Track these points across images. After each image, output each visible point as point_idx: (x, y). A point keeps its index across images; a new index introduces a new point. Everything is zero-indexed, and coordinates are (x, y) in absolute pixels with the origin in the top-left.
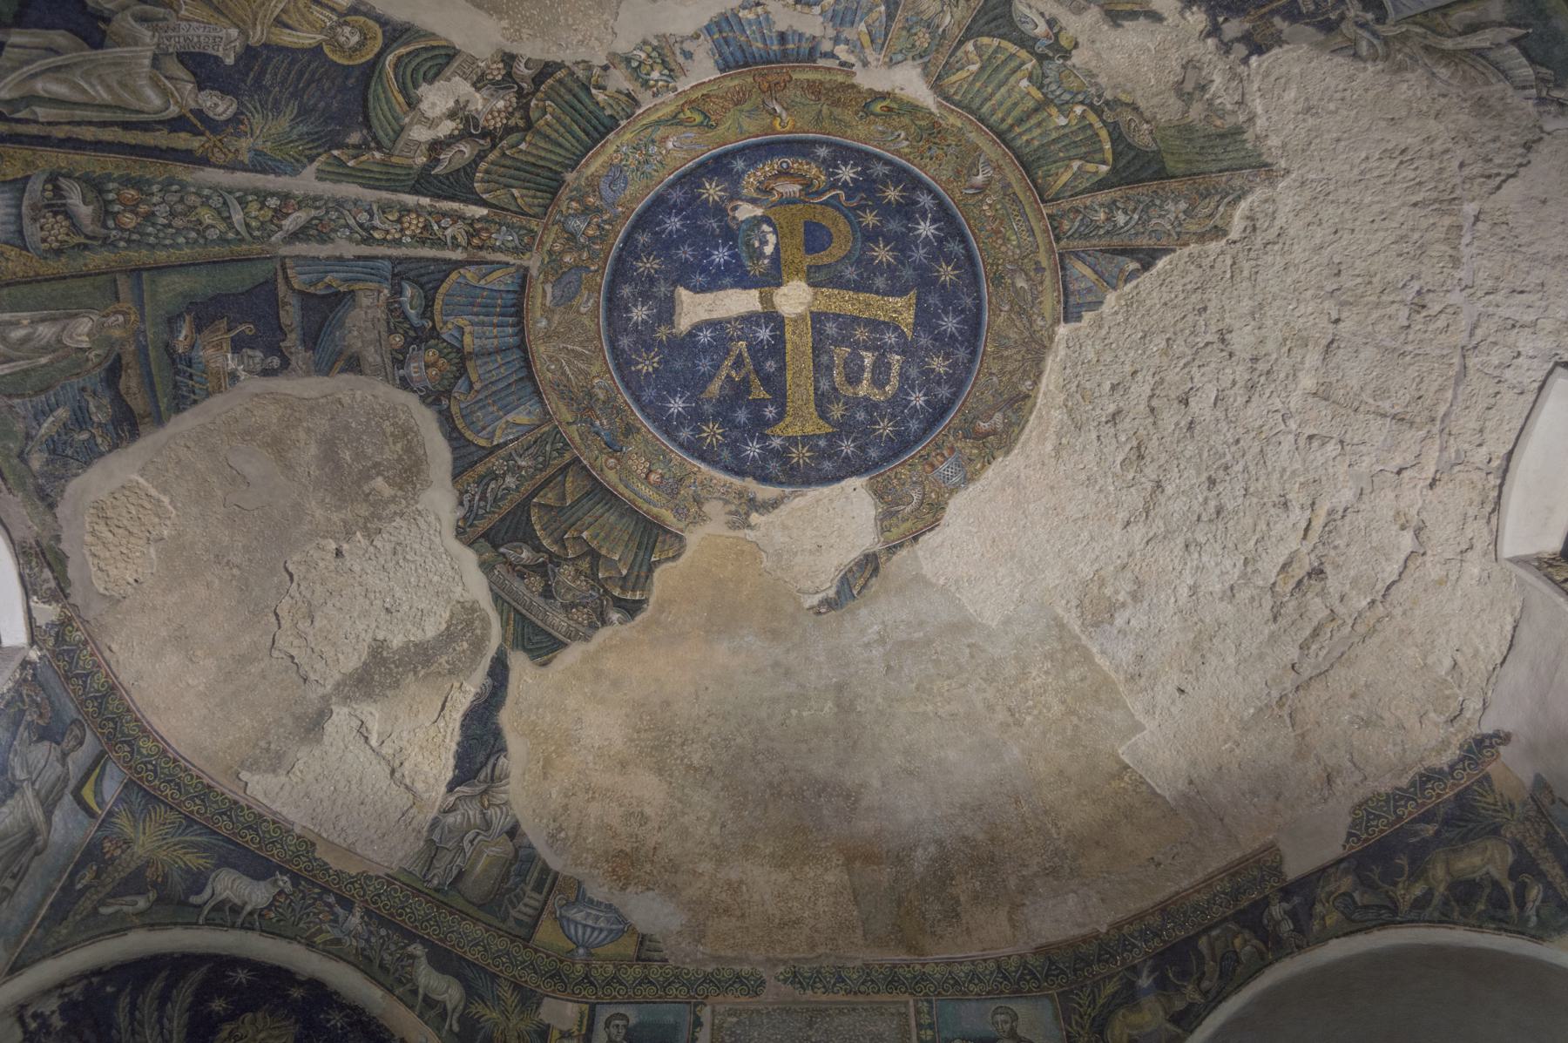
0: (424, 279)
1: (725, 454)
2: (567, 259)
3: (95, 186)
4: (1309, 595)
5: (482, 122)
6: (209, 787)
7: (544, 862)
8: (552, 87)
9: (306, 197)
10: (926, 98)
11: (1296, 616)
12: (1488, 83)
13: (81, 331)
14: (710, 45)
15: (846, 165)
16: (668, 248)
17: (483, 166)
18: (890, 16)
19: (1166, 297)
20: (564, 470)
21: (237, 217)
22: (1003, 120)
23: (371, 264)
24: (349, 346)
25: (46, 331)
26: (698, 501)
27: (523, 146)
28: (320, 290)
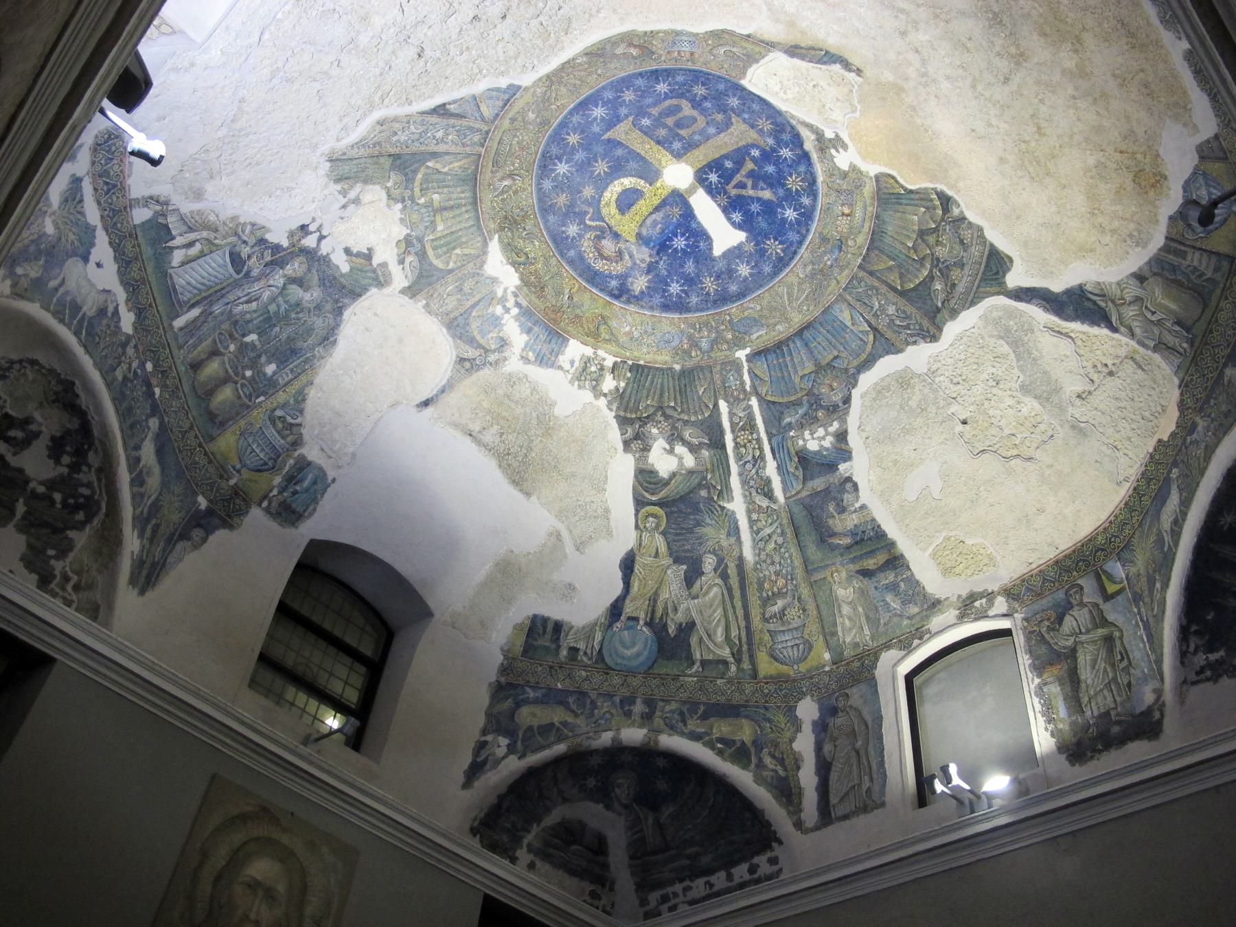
0: (777, 414)
1: (802, 168)
3: (766, 601)
6: (1126, 504)
7: (1160, 249)
8: (631, 412)
10: (494, 247)
12: (192, 212)
13: (844, 593)
14: (561, 358)
15: (568, 237)
16: (692, 279)
18: (473, 306)
19: (443, 81)
20: (871, 274)
21: (768, 531)
25: (846, 610)
26: (845, 175)
27: (672, 404)
28: (800, 473)
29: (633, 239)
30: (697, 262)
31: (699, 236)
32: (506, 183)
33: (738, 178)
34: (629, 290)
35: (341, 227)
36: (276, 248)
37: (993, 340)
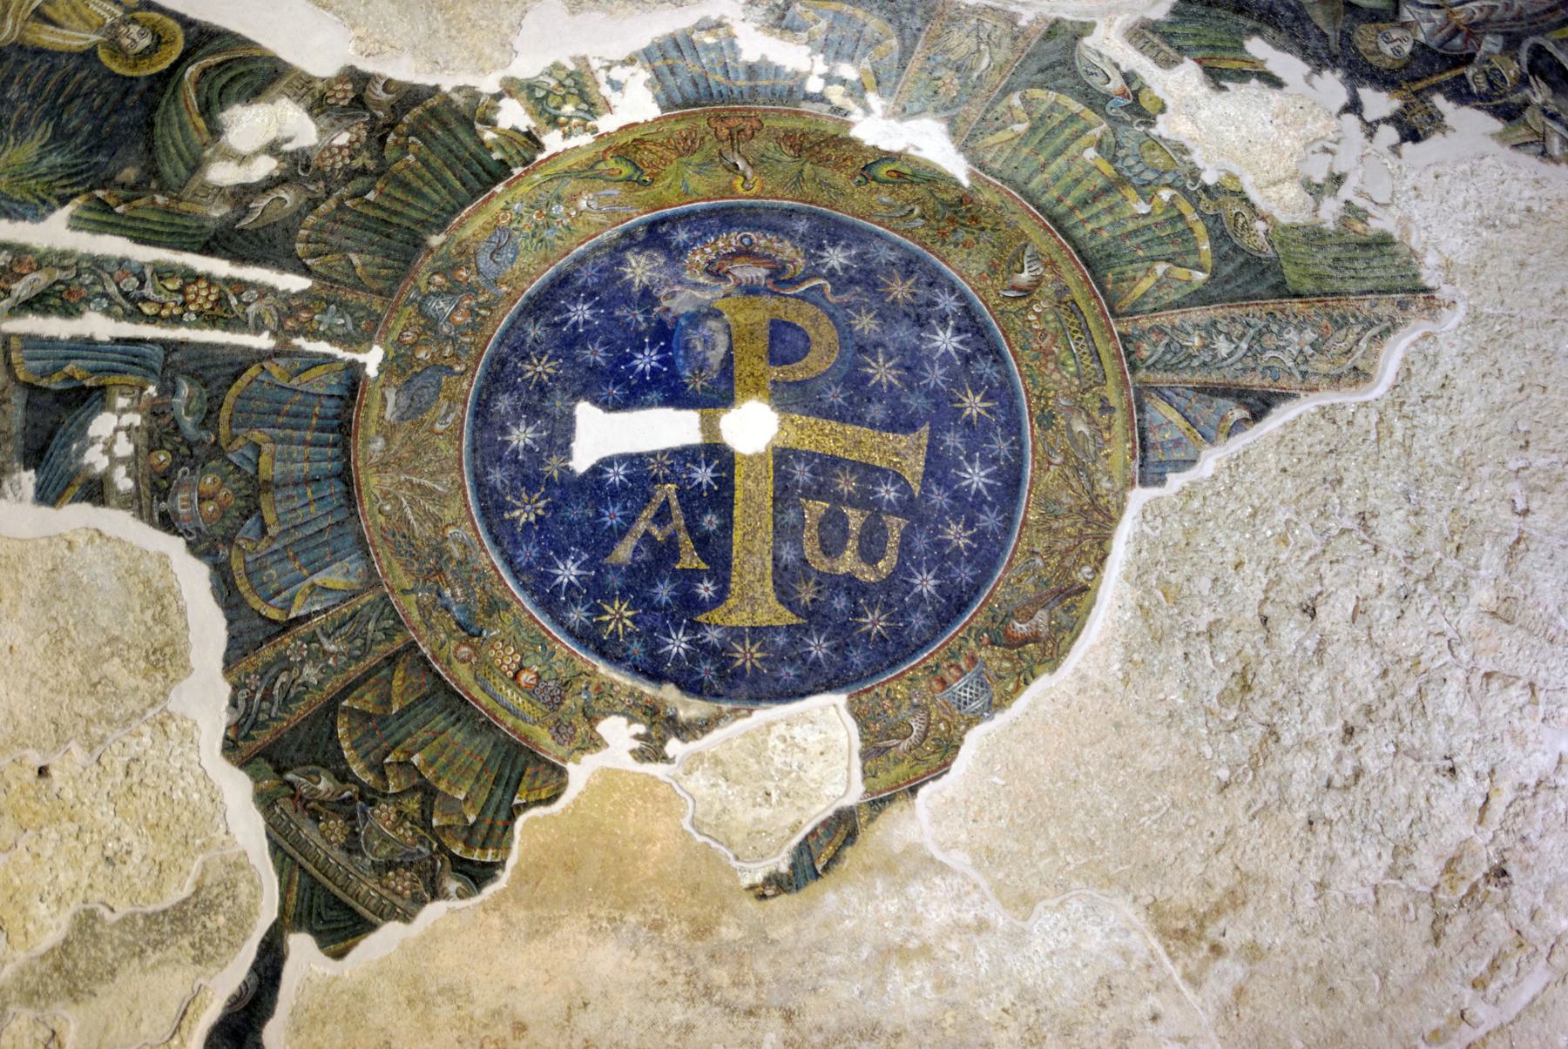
0: (210, 374)
1: (636, 648)
2: (422, 354)
4: (1487, 907)
5: (314, 163)
8: (420, 119)
9: (50, 251)
10: (957, 167)
11: (1466, 938)
14: (644, 75)
15: (834, 244)
17: (311, 219)
18: (906, 53)
19: (1286, 464)
20: (391, 660)
22: (1059, 200)
23: (134, 349)
24: (91, 465)
26: (591, 718)
27: (371, 196)
28: (56, 383)
29: (719, 305)
30: (593, 369)
31: (629, 393)
32: (1025, 277)
33: (678, 519)
34: (647, 248)
35: (1319, 126)
36: (1461, 94)
37: (195, 869)
